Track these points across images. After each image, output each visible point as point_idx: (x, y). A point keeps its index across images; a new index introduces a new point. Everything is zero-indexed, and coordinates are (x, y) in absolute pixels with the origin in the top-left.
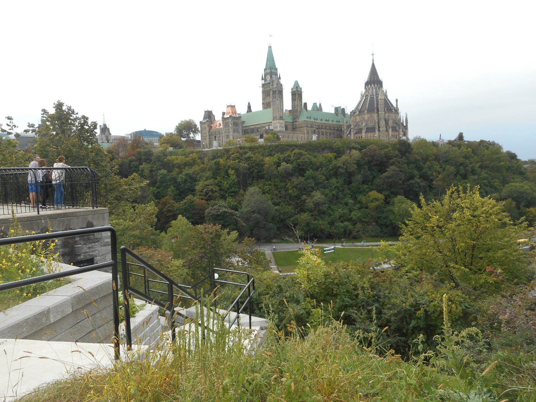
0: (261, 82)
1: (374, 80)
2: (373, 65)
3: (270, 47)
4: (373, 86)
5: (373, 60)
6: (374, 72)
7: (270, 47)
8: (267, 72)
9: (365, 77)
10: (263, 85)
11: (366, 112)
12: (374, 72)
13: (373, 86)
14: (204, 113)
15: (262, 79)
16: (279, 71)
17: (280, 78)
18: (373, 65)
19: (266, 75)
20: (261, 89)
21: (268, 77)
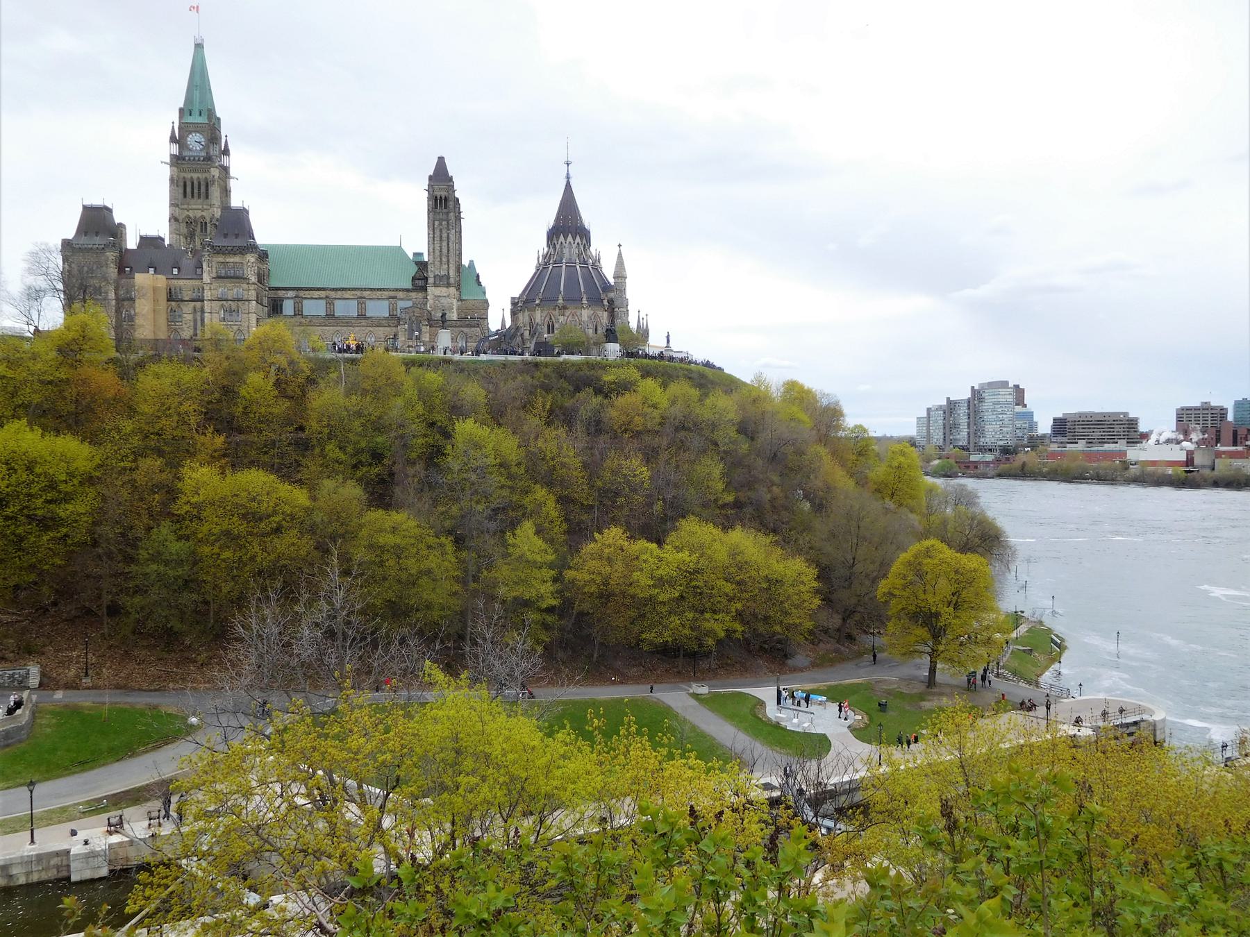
0: (167, 150)
1: (568, 225)
2: (568, 187)
3: (199, 46)
4: (570, 238)
5: (568, 177)
6: (568, 207)
7: (199, 46)
8: (190, 120)
9: (548, 215)
10: (176, 161)
11: (585, 301)
12: (568, 207)
13: (570, 238)
15: (173, 139)
16: (224, 132)
17: (226, 152)
18: (568, 187)
19: (185, 129)
20: (166, 171)
21: (195, 141)
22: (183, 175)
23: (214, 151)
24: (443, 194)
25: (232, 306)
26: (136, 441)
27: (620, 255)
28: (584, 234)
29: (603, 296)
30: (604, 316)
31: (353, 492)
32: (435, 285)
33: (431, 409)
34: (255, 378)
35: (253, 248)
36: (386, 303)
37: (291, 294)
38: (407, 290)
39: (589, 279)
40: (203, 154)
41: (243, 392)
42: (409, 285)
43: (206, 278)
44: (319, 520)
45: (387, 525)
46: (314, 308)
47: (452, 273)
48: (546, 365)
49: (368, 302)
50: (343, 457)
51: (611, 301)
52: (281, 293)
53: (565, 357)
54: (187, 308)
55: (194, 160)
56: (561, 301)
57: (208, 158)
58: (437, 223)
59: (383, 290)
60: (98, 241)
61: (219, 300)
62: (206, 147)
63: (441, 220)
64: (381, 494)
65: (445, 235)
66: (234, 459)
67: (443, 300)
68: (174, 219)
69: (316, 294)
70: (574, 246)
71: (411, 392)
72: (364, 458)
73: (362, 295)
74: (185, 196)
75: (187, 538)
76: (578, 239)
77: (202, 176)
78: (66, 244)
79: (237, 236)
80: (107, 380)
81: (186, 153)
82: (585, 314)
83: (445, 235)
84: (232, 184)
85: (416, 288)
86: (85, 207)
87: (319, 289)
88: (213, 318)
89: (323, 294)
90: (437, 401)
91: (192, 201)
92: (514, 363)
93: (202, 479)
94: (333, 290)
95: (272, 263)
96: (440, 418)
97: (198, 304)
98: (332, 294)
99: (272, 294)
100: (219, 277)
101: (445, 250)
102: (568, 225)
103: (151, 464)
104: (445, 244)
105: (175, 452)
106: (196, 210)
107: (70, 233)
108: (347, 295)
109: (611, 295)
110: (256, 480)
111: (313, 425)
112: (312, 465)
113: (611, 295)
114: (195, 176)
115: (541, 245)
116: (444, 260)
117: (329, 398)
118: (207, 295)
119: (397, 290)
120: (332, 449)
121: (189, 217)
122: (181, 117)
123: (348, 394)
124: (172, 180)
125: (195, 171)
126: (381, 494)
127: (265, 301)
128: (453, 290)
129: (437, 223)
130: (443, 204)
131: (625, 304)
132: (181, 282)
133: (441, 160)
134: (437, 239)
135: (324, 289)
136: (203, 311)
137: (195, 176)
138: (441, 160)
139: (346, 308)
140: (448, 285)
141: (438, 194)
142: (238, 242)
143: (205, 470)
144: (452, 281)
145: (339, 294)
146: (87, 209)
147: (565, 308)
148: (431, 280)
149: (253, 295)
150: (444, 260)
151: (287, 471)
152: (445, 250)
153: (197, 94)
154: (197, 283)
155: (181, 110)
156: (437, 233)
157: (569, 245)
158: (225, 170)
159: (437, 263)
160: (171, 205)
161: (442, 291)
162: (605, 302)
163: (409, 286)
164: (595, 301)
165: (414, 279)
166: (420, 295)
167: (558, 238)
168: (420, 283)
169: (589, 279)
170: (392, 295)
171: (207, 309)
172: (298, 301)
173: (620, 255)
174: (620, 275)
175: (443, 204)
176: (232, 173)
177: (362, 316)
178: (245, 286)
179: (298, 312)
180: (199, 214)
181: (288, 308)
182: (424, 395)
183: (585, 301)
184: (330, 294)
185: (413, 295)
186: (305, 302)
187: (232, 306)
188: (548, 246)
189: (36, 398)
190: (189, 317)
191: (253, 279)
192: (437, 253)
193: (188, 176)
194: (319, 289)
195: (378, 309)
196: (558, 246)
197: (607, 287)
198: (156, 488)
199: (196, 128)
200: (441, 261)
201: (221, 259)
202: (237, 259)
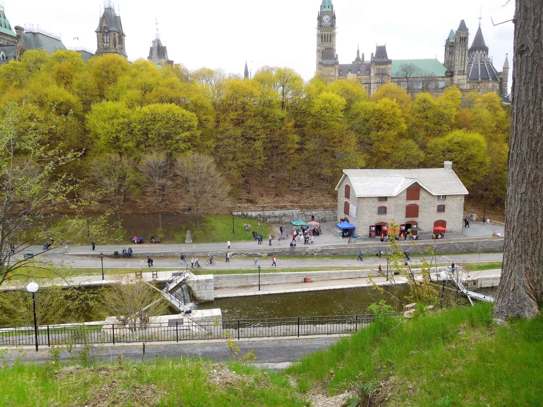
0: (315, 23)
2: (479, 29)
8: (324, 10)
11: (490, 79)
13: (481, 52)
21: (326, 18)
22: (324, 33)
24: (464, 36)
32: (459, 75)
35: (390, 62)
38: (443, 77)
40: (330, 24)
42: (444, 75)
43: (372, 74)
47: (466, 69)
51: (501, 79)
55: (326, 27)
56: (480, 80)
65: (464, 53)
67: (461, 81)
70: (483, 55)
74: (322, 41)
81: (323, 24)
83: (464, 53)
85: (447, 76)
91: (325, 44)
97: (368, 85)
101: (463, 60)
104: (463, 57)
113: (501, 76)
116: (463, 64)
118: (372, 81)
124: (318, 36)
125: (326, 31)
128: (465, 76)
132: (361, 77)
133: (463, 22)
134: (460, 55)
137: (326, 33)
138: (463, 22)
140: (464, 74)
141: (462, 36)
142: (384, 60)
144: (466, 72)
150: (463, 64)
154: (368, 77)
155: (321, 6)
156: (461, 53)
159: (460, 65)
160: (318, 45)
161: (461, 77)
162: (499, 80)
163: (444, 75)
164: (495, 79)
165: (446, 72)
166: (449, 79)
168: (449, 74)
169: (483, 68)
183: (490, 79)
185: (446, 79)
193: (324, 33)
196: (475, 55)
199: (327, 13)
201: (378, 67)
202: (384, 67)
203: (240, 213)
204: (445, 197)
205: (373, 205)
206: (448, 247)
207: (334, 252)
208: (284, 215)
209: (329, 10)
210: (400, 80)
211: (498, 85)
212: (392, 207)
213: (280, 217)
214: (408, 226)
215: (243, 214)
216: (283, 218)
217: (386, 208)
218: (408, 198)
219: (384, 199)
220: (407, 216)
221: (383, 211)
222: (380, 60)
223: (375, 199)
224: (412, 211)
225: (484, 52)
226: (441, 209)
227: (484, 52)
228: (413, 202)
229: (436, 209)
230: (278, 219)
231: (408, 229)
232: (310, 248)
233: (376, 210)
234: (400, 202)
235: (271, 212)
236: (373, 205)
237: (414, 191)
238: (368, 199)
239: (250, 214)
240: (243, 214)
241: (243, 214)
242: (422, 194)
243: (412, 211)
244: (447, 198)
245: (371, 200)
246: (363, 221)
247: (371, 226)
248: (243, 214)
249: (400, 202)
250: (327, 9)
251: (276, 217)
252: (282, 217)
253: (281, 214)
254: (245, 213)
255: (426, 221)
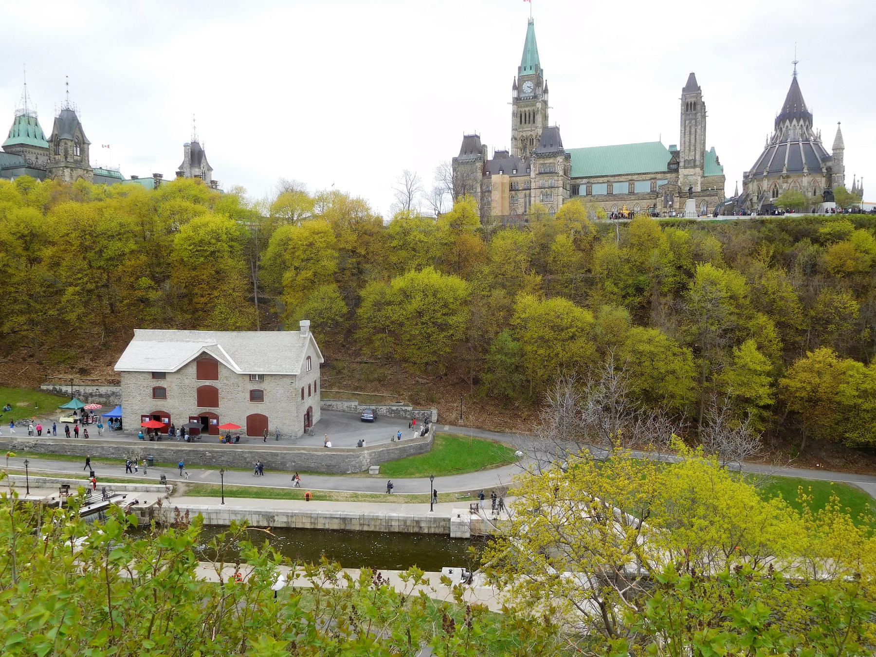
0: (510, 94)
1: (794, 111)
2: (795, 82)
3: (531, 24)
4: (795, 122)
5: (795, 74)
7: (531, 24)
8: (524, 73)
10: (517, 101)
11: (805, 171)
13: (795, 122)
14: (462, 139)
15: (515, 88)
17: (546, 91)
18: (795, 82)
19: (522, 79)
20: (509, 109)
21: (528, 86)
23: (539, 91)
24: (693, 100)
25: (547, 192)
26: (491, 279)
27: (839, 131)
28: (806, 117)
29: (822, 165)
30: (822, 182)
31: (622, 314)
32: (685, 167)
33: (679, 256)
34: (561, 238)
35: (562, 152)
36: (649, 183)
37: (584, 181)
38: (664, 173)
39: (810, 153)
40: (532, 94)
41: (554, 248)
42: (666, 169)
43: (533, 175)
44: (599, 332)
45: (645, 338)
46: (599, 189)
47: (698, 157)
48: (771, 222)
49: (636, 183)
50: (616, 290)
51: (829, 169)
52: (578, 181)
53: (787, 215)
54: (521, 195)
56: (785, 172)
57: (535, 97)
58: (687, 122)
59: (647, 173)
60: (472, 157)
61: (540, 188)
62: (534, 90)
63: (690, 120)
64: (642, 316)
65: (693, 130)
66: (548, 291)
67: (690, 178)
68: (514, 138)
69: (601, 180)
70: (798, 128)
71: (665, 244)
72: (631, 291)
73: (631, 178)
75: (518, 340)
76: (802, 122)
77: (531, 109)
78: (455, 160)
79: (552, 146)
80: (475, 241)
81: (522, 95)
82: (805, 181)
83: (693, 130)
84: (550, 112)
86: (465, 137)
87: (602, 177)
88: (536, 200)
89: (605, 179)
90: (684, 251)
92: (744, 221)
93: (528, 303)
94: (612, 176)
95: (573, 162)
96: (686, 263)
97: (528, 192)
98: (612, 179)
99: (573, 182)
100: (540, 173)
101: (693, 141)
102: (794, 111)
103: (499, 293)
104: (693, 136)
105: (513, 286)
106: (528, 131)
107: (457, 155)
108: (621, 179)
109: (830, 164)
110: (560, 304)
111: (597, 268)
112: (596, 296)
113: (830, 164)
114: (527, 109)
115: (769, 130)
116: (692, 148)
117: (608, 250)
118: (533, 185)
119: (656, 173)
120: (608, 284)
121: (522, 136)
122: (519, 73)
123: (621, 247)
124: (514, 114)
126: (642, 316)
127: (568, 187)
128: (698, 170)
129: (687, 122)
130: (693, 107)
131: (842, 170)
132: (518, 179)
133: (692, 76)
134: (687, 133)
135: (606, 176)
136: (530, 196)
137: (527, 109)
138: (692, 76)
139: (621, 188)
140: (695, 167)
141: (689, 101)
143: (530, 297)
144: (698, 163)
145: (617, 179)
146: (465, 137)
147: (788, 177)
148: (682, 164)
149: (560, 183)
150: (692, 148)
151: (580, 299)
152: (693, 141)
153: (529, 56)
154: (527, 178)
155: (520, 68)
156: (688, 129)
157: (794, 128)
158: (545, 103)
159: (687, 151)
160: (513, 130)
161: (690, 171)
162: (824, 170)
163: (666, 169)
164: (815, 169)
165: (669, 164)
166: (674, 175)
167: (784, 122)
168: (673, 167)
169: (810, 153)
170: (653, 177)
171: (533, 195)
172: (589, 185)
173: (839, 131)
174: (839, 147)
175: (693, 107)
176: (550, 104)
177: (632, 193)
178: (556, 178)
179: (589, 193)
180: (529, 134)
181: (583, 190)
182: (674, 246)
183: (805, 171)
184: (610, 179)
185: (669, 175)
186: (594, 186)
187: (547, 192)
188: (776, 130)
189: (439, 254)
190: (522, 200)
191: (561, 173)
192: (687, 143)
193: (523, 110)
194: (602, 177)
195: (643, 187)
196: (784, 129)
197: (826, 158)
198: (501, 308)
200: (690, 150)
201: (541, 162)
202: (551, 161)
203: (51, 387)
204: (262, 377)
205: (145, 383)
206: (231, 458)
207: (51, 448)
208: (113, 393)
209: (532, 72)
210: (635, 177)
211: (824, 180)
212: (176, 388)
213: (108, 396)
214: (204, 420)
215: (55, 389)
216: (111, 399)
217: (164, 389)
218: (200, 376)
219: (158, 375)
220: (200, 404)
221: (159, 393)
222: (544, 150)
223: (147, 375)
224: (208, 397)
225: (807, 123)
226: (256, 396)
227: (807, 123)
228: (207, 383)
229: (248, 396)
230: (104, 400)
231: (204, 425)
232: (19, 440)
233: (150, 391)
234: (187, 382)
235: (95, 388)
236: (145, 383)
237: (206, 365)
238: (136, 374)
239: (64, 389)
240: (54, 388)
241: (55, 389)
242: (222, 373)
243: (208, 397)
244: (267, 381)
245: (140, 377)
246: (135, 406)
247: (143, 416)
248: (54, 388)
249: (187, 382)
250: (529, 72)
251: (101, 396)
252: (109, 396)
253: (109, 393)
254: (58, 387)
255: (233, 412)
